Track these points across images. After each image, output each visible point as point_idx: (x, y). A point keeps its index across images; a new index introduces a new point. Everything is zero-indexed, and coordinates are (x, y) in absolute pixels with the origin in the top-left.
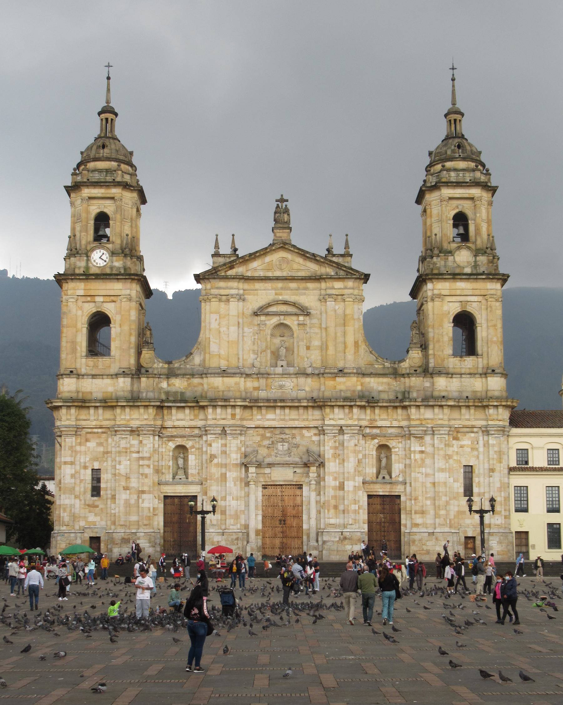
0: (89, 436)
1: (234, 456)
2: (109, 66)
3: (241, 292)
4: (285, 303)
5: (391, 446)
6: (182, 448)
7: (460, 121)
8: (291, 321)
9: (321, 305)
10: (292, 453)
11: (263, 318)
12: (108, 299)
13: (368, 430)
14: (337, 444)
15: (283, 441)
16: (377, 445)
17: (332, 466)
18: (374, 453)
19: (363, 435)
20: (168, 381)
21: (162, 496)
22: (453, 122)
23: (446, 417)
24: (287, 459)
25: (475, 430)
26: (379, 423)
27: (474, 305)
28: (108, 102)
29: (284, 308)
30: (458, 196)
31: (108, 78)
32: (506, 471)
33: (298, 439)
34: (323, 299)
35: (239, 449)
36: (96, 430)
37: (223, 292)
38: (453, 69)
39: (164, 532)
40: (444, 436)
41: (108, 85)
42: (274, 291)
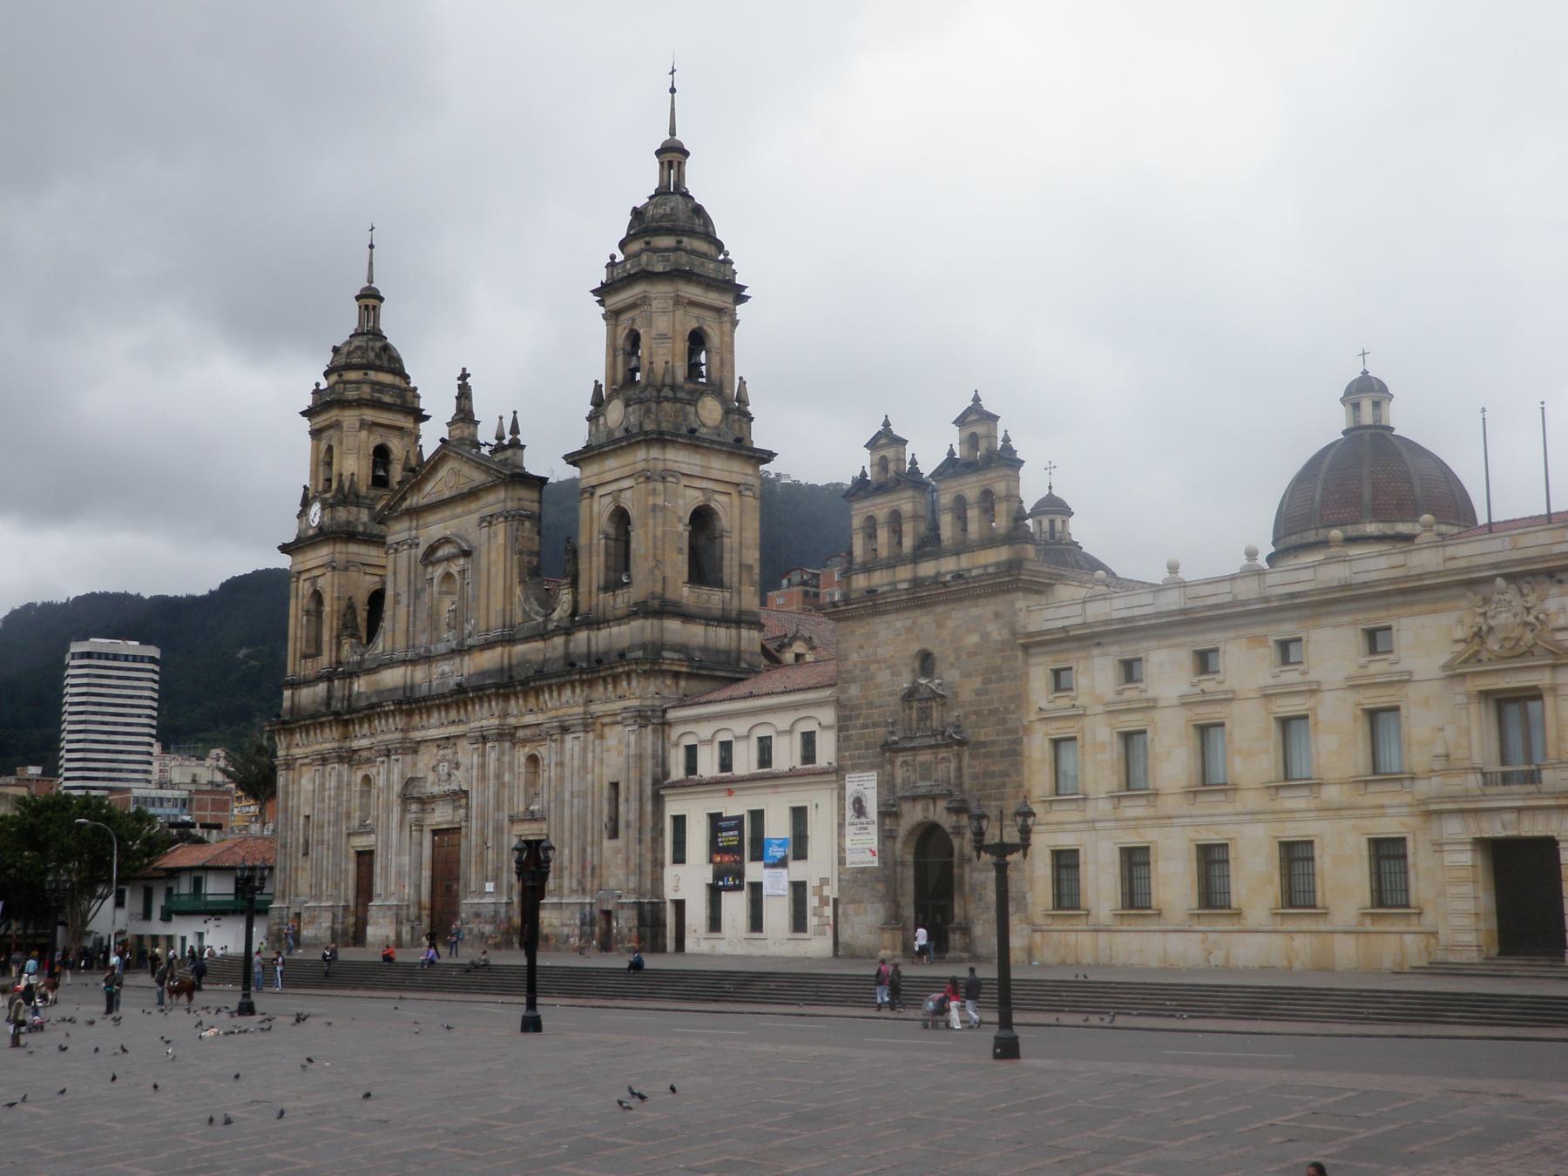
0: (304, 769)
2: (371, 230)
4: (446, 540)
6: (367, 780)
7: (679, 163)
8: (454, 569)
11: (430, 569)
13: (520, 734)
15: (443, 759)
17: (474, 795)
18: (523, 770)
21: (352, 852)
22: (666, 166)
23: (581, 701)
24: (446, 787)
25: (619, 718)
26: (529, 719)
27: (628, 494)
28: (370, 281)
30: (621, 305)
31: (371, 247)
32: (648, 791)
33: (462, 758)
35: (402, 774)
38: (672, 73)
39: (357, 905)
41: (371, 256)
42: (442, 525)
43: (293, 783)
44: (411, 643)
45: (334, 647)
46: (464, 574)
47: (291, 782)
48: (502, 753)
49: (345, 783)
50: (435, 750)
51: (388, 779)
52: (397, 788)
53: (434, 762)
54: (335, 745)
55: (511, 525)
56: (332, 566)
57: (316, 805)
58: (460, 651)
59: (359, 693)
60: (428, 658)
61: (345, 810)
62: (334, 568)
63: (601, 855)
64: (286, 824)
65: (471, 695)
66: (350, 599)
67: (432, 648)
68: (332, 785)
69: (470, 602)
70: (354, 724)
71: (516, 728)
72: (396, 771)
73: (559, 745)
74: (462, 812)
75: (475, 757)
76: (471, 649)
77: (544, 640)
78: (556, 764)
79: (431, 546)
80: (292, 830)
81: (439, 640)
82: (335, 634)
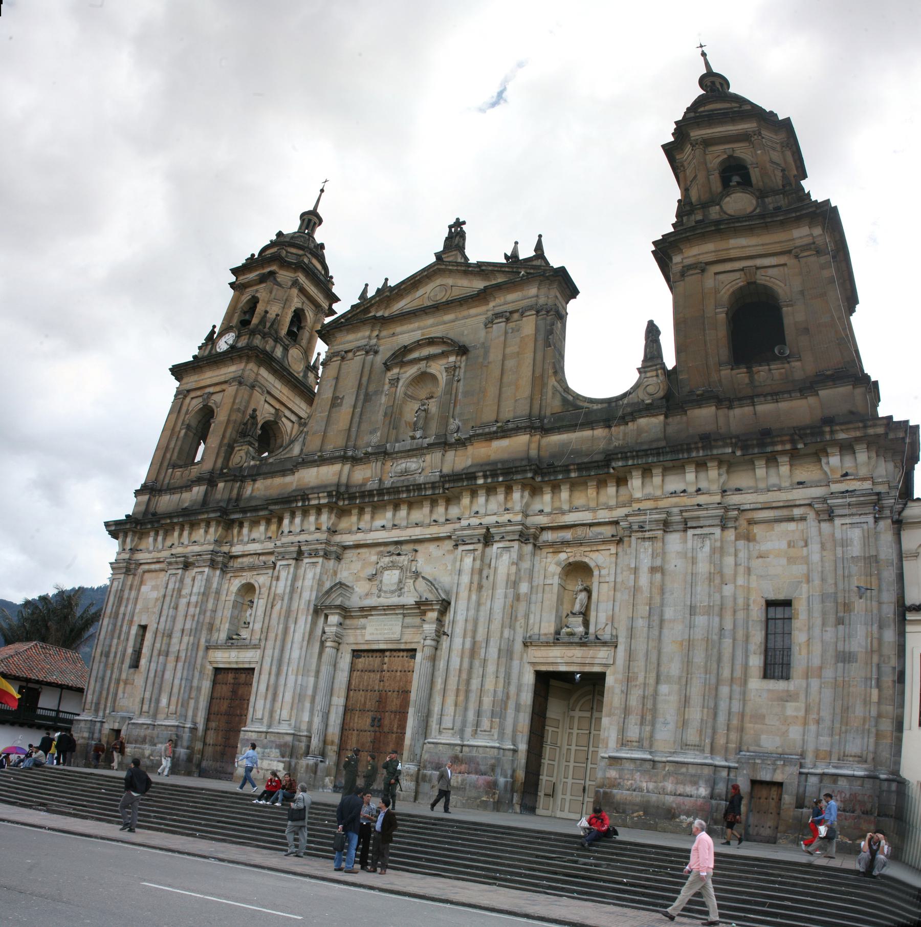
0: (147, 575)
1: (306, 595)
3: (374, 341)
4: (431, 342)
5: (592, 564)
6: (249, 588)
8: (437, 368)
9: (487, 333)
10: (406, 589)
11: (396, 371)
12: (218, 388)
13: (548, 536)
14: (478, 563)
15: (393, 566)
16: (563, 564)
18: (556, 581)
19: (535, 545)
20: (254, 484)
24: (394, 600)
27: (771, 272)
29: (426, 351)
33: (421, 564)
34: (489, 323)
35: (320, 583)
36: (153, 567)
37: (348, 347)
40: (711, 530)
42: (420, 332)
43: (131, 589)
44: (351, 443)
45: (222, 454)
46: (454, 370)
47: (128, 587)
48: (521, 557)
49: (214, 590)
50: (374, 558)
51: (292, 585)
52: (308, 594)
53: (371, 570)
54: (211, 547)
55: (545, 319)
56: (240, 381)
57: (165, 613)
58: (443, 444)
59: (251, 498)
60: (383, 454)
61: (207, 620)
62: (240, 383)
63: (744, 701)
64: (113, 631)
65: (480, 481)
66: (255, 410)
67: (388, 445)
68: (195, 590)
69: (460, 396)
70: (241, 525)
71: (543, 529)
72: (310, 575)
73: (660, 544)
74: (430, 628)
75: (468, 561)
76: (461, 443)
77: (609, 427)
78: (653, 570)
79: (405, 347)
80: (119, 638)
81: (397, 441)
82: (226, 441)
